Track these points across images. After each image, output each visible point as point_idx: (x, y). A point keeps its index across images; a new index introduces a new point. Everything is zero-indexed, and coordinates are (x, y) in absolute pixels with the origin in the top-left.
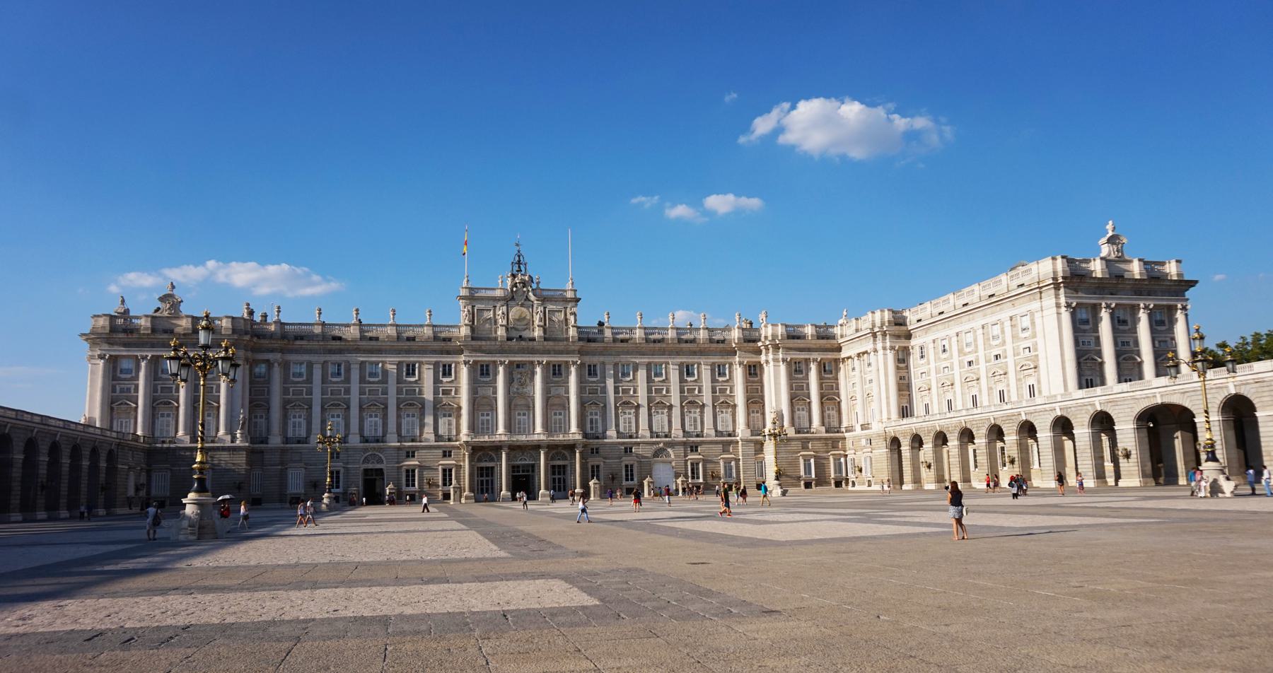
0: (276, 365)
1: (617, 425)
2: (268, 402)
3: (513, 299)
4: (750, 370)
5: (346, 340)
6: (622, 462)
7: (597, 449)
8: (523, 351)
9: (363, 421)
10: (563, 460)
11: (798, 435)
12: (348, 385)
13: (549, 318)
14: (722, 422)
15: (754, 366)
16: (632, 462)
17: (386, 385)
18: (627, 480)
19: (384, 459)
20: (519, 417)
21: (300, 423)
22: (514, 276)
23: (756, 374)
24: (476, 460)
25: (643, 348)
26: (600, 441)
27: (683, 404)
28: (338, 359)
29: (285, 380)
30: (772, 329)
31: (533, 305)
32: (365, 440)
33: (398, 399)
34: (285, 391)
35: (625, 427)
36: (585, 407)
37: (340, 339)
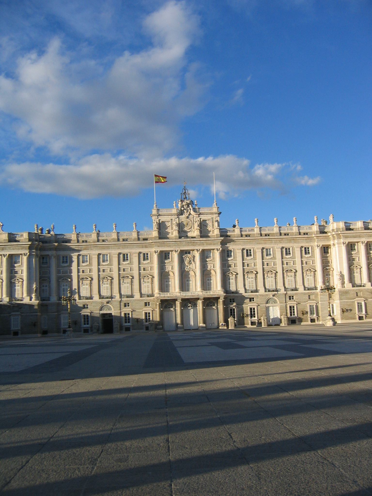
0: (53, 257)
1: (244, 285)
2: (49, 278)
4: (324, 250)
5: (89, 242)
7: (233, 299)
12: (92, 267)
19: (112, 308)
22: (182, 201)
24: (163, 307)
27: (284, 272)
28: (86, 253)
29: (58, 266)
30: (337, 225)
31: (193, 217)
32: (101, 297)
34: (58, 272)
35: (250, 286)
37: (86, 242)
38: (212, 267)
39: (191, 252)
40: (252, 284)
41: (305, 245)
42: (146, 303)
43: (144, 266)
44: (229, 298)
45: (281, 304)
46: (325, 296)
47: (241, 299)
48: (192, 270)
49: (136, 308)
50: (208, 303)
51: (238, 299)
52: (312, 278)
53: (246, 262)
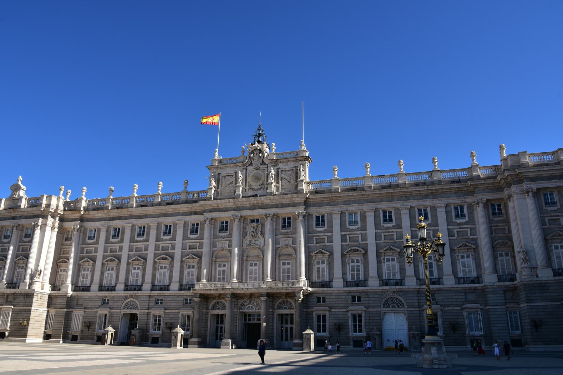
3: (251, 164)
6: (348, 311)
7: (324, 298)
8: (253, 207)
9: (129, 273)
10: (289, 309)
11: (557, 278)
13: (281, 177)
14: (464, 266)
15: (499, 206)
16: (359, 312)
17: (147, 243)
18: (355, 331)
19: (139, 305)
20: (251, 267)
21: (87, 275)
23: (501, 213)
24: (210, 307)
25: (369, 195)
26: (325, 289)
31: (267, 168)
33: (155, 254)
35: (353, 275)
36: (312, 256)
38: (291, 243)
39: (260, 220)
40: (357, 271)
41: (453, 201)
42: (186, 300)
43: (191, 243)
44: (315, 295)
45: (411, 309)
46: (497, 295)
47: (338, 297)
48: (259, 248)
49: (170, 306)
50: (281, 304)
51: (332, 297)
52: (470, 262)
53: (348, 234)
